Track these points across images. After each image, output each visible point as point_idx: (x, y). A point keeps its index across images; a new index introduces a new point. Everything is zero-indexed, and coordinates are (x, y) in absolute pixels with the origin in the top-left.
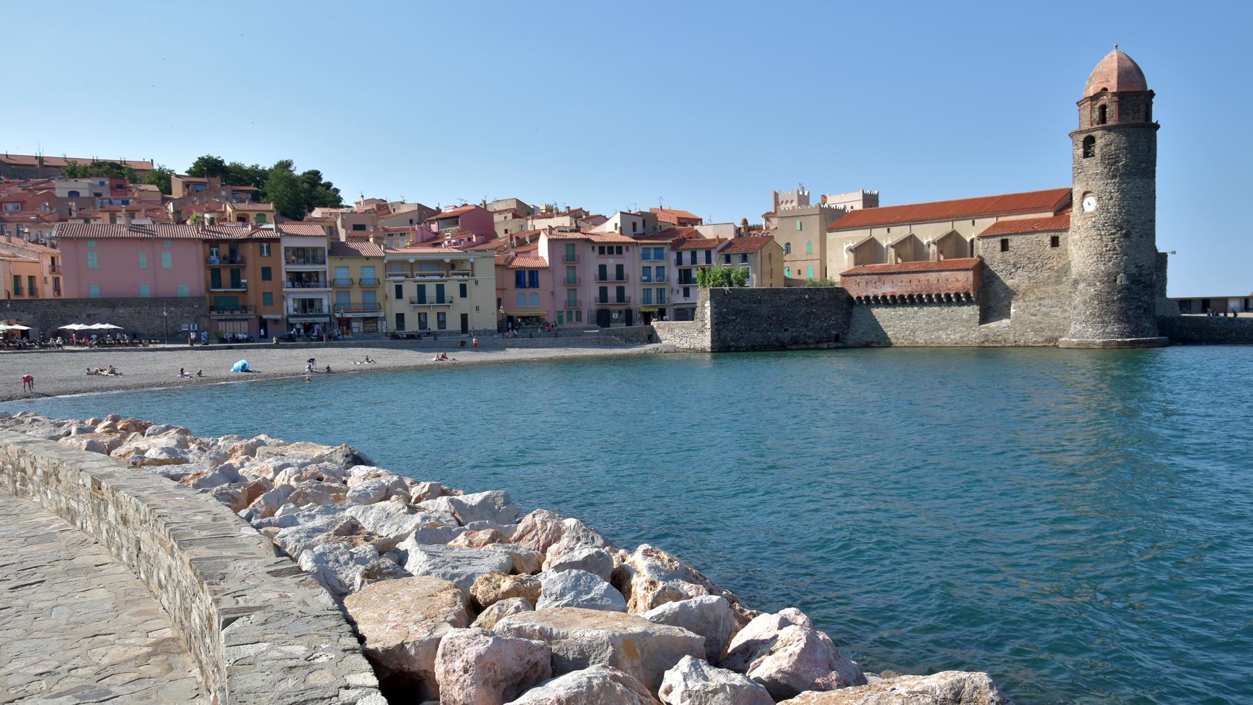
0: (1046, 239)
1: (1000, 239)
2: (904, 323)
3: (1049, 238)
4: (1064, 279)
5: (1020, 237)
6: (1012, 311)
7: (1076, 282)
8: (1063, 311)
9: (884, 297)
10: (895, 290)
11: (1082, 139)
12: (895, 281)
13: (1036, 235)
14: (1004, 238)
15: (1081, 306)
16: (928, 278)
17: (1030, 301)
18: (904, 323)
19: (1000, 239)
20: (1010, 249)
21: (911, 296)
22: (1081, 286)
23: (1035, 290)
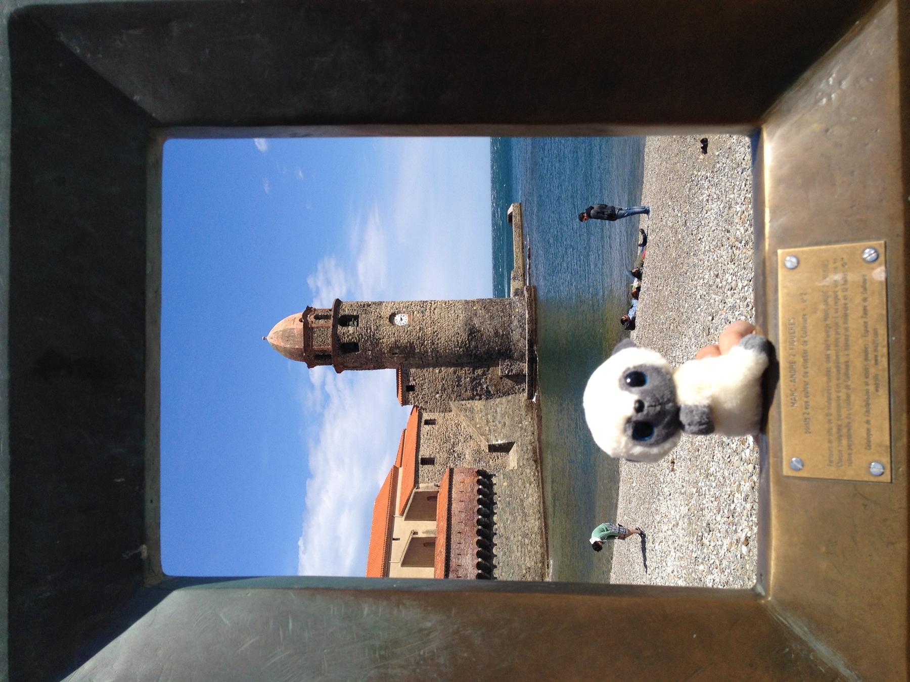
0: (427, 427)
1: (420, 466)
2: (515, 548)
3: (425, 426)
4: (469, 406)
5: (422, 448)
6: (500, 442)
7: (473, 332)
8: (501, 404)
9: (479, 566)
10: (470, 551)
11: (339, 327)
12: (458, 552)
13: (422, 436)
14: (420, 461)
15: (495, 322)
16: (457, 513)
17: (490, 430)
18: (515, 548)
19: (420, 466)
20: (432, 456)
21: (479, 533)
22: (476, 322)
23: (478, 426)
